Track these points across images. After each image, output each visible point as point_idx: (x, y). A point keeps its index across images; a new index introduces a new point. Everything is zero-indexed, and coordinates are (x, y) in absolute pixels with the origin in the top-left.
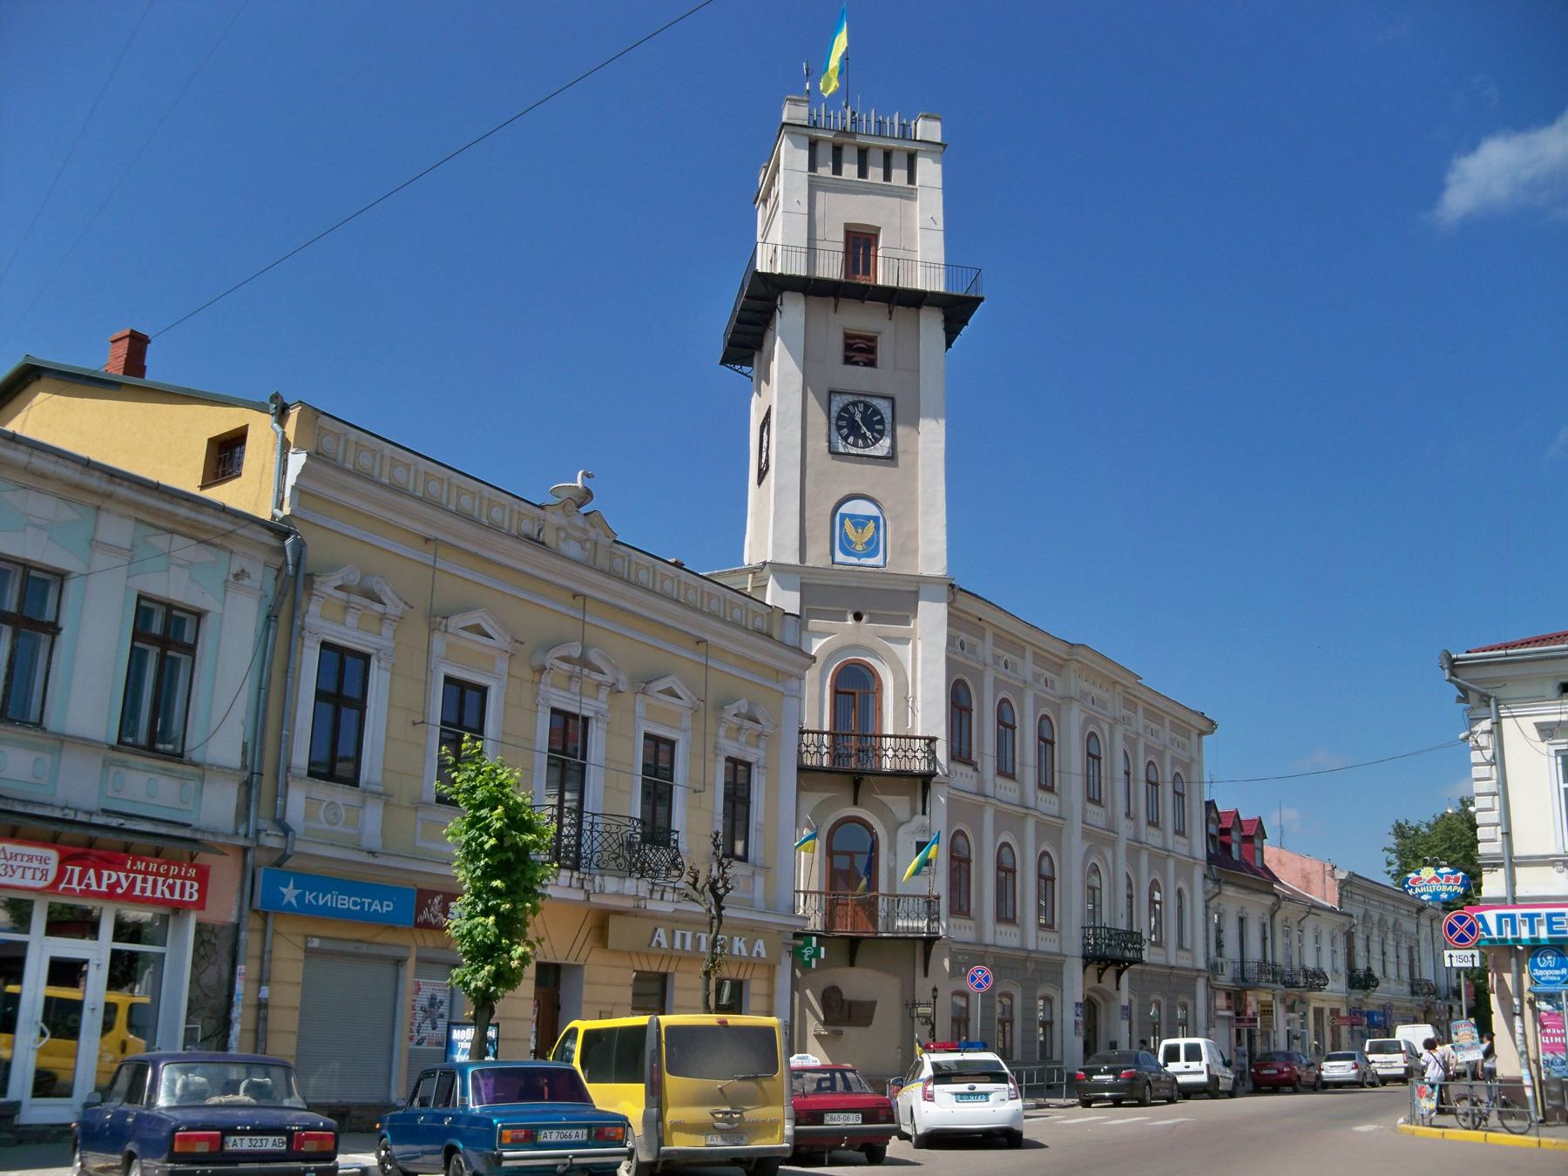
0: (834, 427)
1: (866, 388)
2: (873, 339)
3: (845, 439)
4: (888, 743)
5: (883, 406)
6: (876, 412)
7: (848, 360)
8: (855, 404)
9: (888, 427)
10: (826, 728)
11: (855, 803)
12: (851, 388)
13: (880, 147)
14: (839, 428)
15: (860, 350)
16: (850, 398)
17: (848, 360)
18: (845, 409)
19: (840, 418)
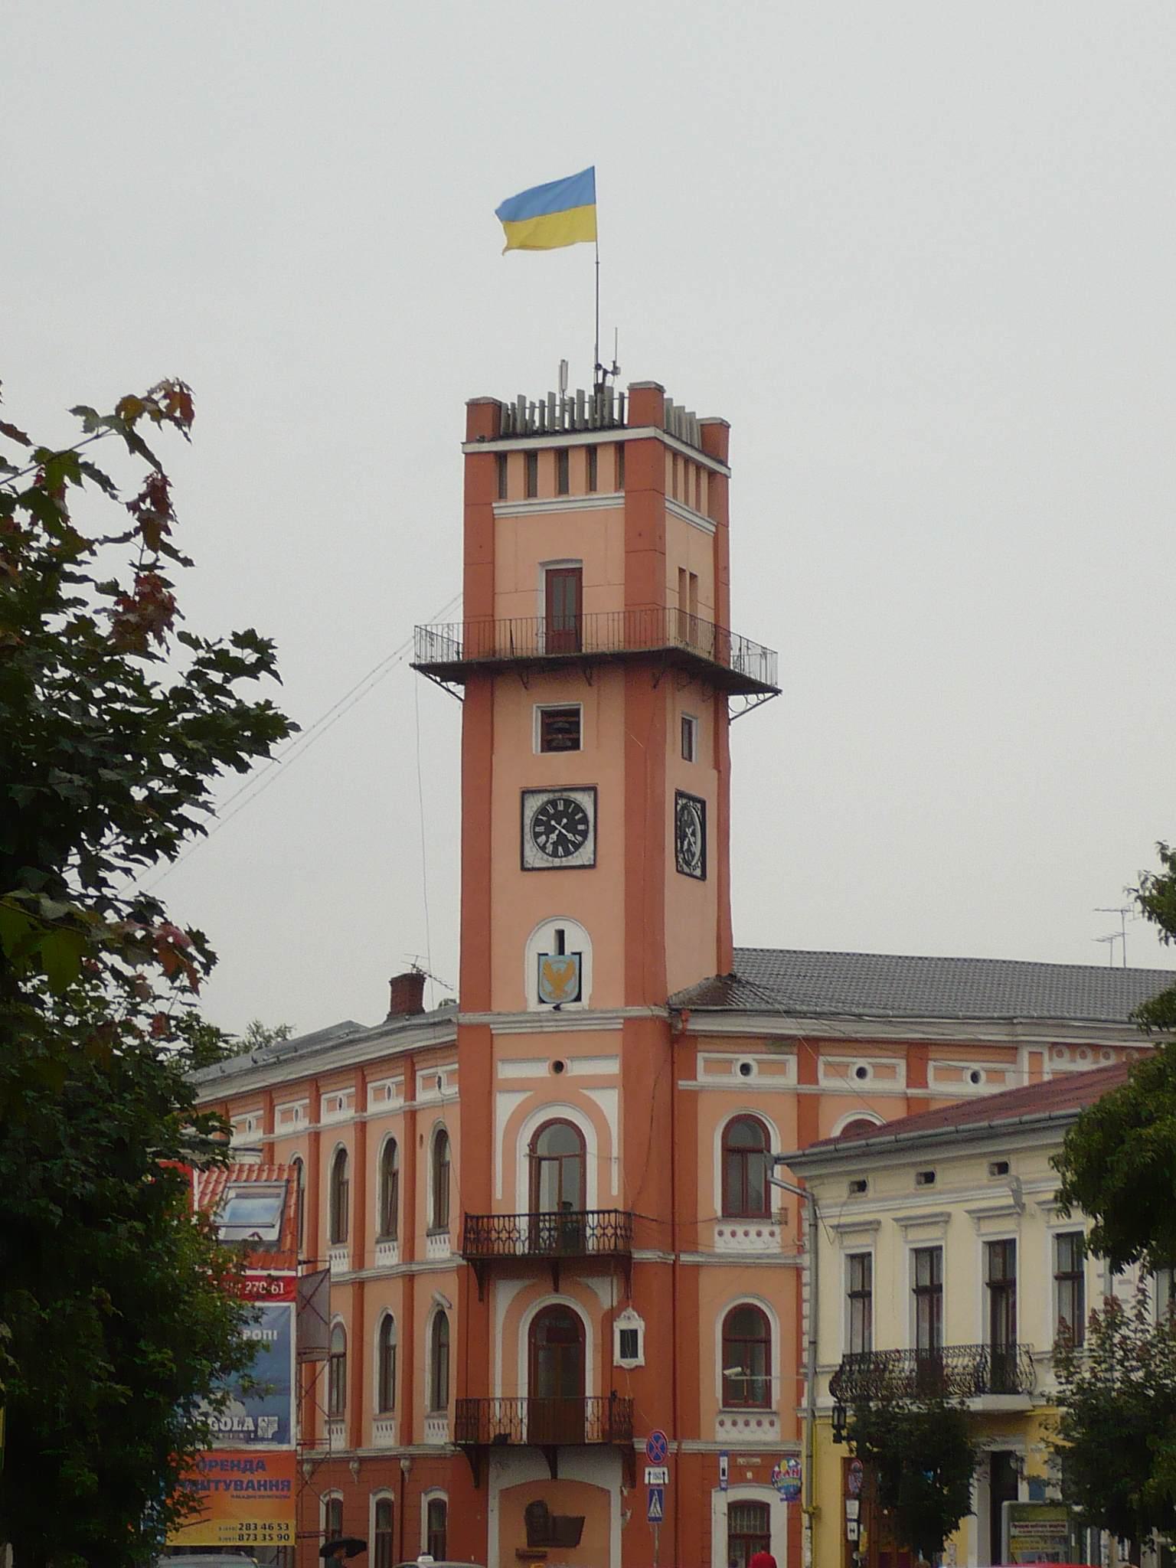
0: (528, 836)
1: (565, 780)
2: (576, 713)
3: (543, 848)
4: (592, 1220)
5: (585, 800)
6: (579, 808)
7: (549, 745)
8: (553, 803)
9: (591, 828)
10: (523, 1206)
11: (556, 1290)
12: (545, 783)
13: (581, 446)
14: (537, 835)
15: (561, 732)
16: (543, 798)
17: (549, 745)
18: (543, 810)
19: (537, 822)
